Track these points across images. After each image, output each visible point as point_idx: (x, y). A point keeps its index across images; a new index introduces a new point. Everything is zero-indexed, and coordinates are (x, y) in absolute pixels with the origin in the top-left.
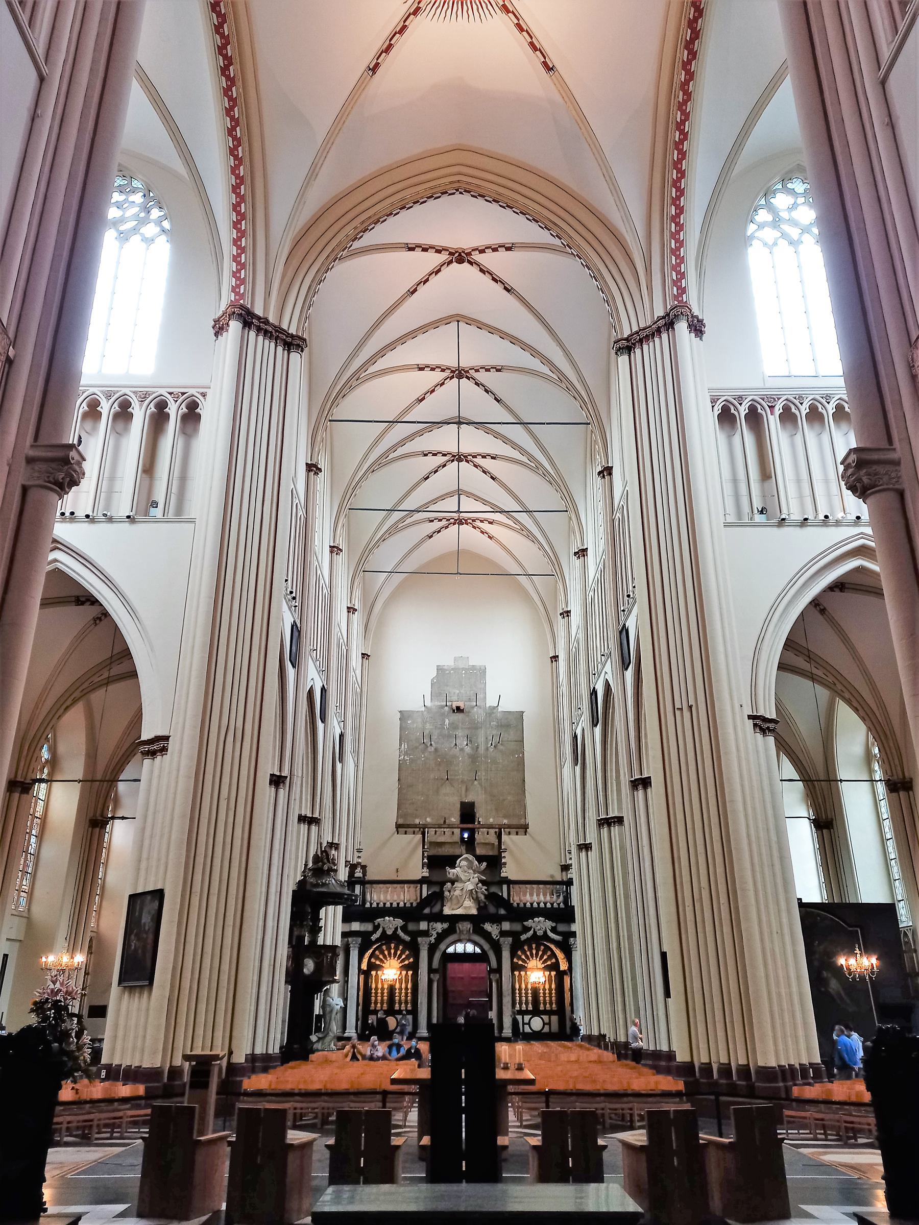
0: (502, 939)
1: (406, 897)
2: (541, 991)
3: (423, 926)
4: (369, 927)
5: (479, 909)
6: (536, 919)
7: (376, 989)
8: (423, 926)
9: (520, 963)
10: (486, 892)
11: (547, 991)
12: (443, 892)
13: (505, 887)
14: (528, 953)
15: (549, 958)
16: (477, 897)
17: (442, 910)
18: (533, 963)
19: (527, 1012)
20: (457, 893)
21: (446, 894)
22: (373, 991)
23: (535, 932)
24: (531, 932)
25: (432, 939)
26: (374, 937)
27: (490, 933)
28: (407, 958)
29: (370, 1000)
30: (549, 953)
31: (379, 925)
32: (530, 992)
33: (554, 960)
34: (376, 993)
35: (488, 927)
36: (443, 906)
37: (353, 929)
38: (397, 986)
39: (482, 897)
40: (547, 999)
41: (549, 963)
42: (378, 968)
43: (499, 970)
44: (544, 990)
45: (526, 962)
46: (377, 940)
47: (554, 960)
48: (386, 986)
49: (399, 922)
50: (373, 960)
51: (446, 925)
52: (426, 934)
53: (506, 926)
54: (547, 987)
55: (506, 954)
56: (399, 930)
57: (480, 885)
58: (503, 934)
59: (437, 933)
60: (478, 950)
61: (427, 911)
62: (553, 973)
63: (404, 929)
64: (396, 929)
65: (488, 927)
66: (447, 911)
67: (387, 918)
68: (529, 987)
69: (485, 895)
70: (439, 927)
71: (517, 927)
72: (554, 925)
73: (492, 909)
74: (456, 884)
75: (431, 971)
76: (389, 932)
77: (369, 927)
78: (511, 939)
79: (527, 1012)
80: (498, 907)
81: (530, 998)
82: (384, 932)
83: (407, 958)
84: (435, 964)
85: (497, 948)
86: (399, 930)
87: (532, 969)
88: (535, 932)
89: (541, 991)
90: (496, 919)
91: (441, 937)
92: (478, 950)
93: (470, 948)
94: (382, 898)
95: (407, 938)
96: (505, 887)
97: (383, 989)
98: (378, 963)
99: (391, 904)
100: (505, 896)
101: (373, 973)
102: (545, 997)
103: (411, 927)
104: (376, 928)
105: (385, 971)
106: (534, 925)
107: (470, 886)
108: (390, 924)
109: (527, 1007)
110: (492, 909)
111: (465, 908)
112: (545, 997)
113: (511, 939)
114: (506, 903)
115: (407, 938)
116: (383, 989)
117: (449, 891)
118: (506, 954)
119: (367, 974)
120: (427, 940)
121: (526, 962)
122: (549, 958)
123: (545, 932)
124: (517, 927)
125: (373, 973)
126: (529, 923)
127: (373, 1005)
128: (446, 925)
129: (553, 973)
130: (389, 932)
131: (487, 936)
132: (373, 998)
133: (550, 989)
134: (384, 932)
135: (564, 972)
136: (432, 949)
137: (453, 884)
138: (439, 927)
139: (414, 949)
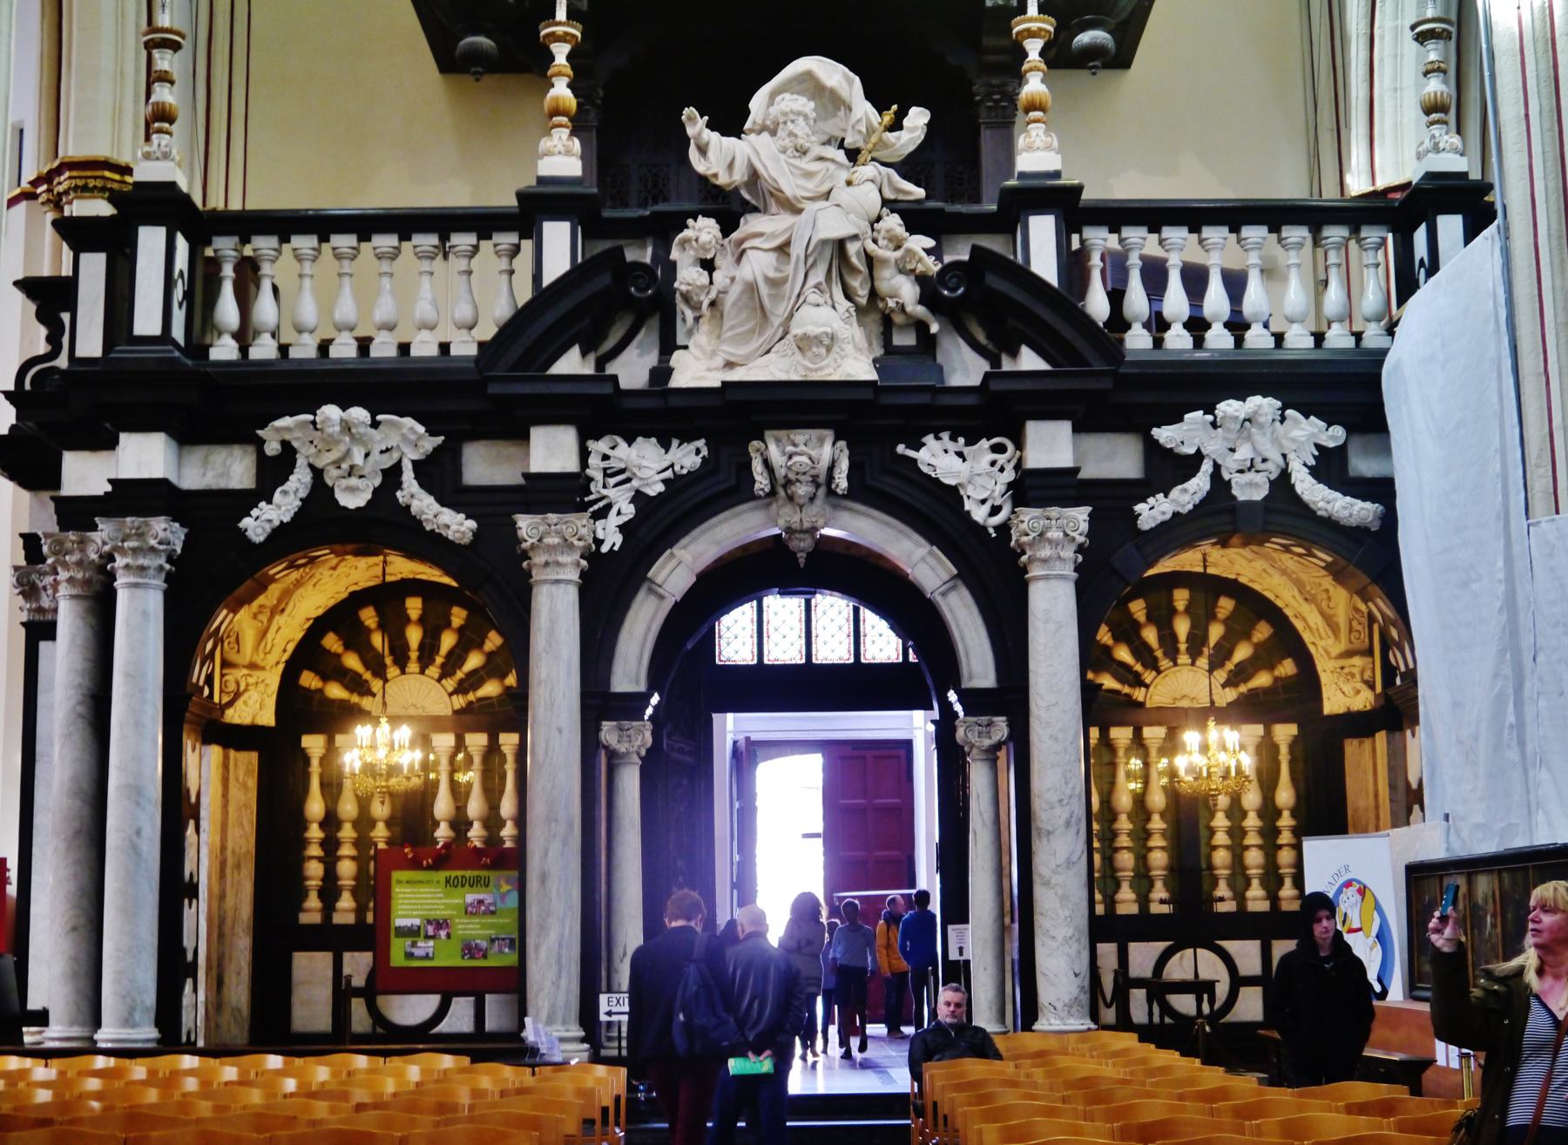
0: (1029, 518)
1: (451, 305)
2: (1220, 821)
3: (552, 450)
4: (231, 468)
5: (889, 356)
6: (1228, 408)
7: (331, 822)
8: (552, 450)
9: (1108, 682)
10: (932, 266)
11: (1252, 821)
12: (672, 266)
13: (1042, 230)
14: (1150, 635)
15: (1263, 658)
16: (874, 294)
17: (661, 373)
18: (1183, 682)
19: (1144, 927)
20: (759, 264)
21: (688, 275)
22: (315, 833)
23: (1219, 484)
24: (1199, 484)
25: (610, 535)
26: (258, 524)
27: (951, 496)
28: (493, 668)
29: (299, 877)
30: (1262, 632)
31: (288, 453)
32: (1157, 824)
33: (1287, 668)
34: (330, 845)
35: (938, 457)
36: (668, 345)
37: (128, 472)
38: (443, 806)
39: (907, 292)
40: (1254, 858)
41: (1262, 680)
42: (333, 719)
43: (1010, 697)
44: (1236, 811)
45: (1138, 682)
46: (281, 534)
47: (1287, 668)
48: (380, 810)
49: (408, 438)
50: (309, 680)
51: (687, 457)
52: (565, 493)
53: (1050, 445)
54: (1252, 799)
55: (1052, 607)
56: (408, 476)
57: (893, 222)
58: (1033, 488)
59: (639, 498)
60: (883, 644)
61: (572, 363)
62: (1285, 733)
63: (439, 474)
64: (392, 476)
65: (938, 457)
66: (695, 369)
67: (330, 412)
68: (1157, 800)
69: (922, 280)
70: (650, 463)
71: (1116, 458)
72: (1334, 436)
73: (964, 367)
74: (750, 224)
75: (599, 703)
76: (353, 497)
77: (231, 468)
78: (1080, 517)
79: (1144, 927)
80: (998, 345)
81: (1158, 859)
82: (320, 491)
83: (493, 668)
84: (629, 669)
85: (997, 575)
86: (408, 476)
87: (1174, 719)
88: (1219, 484)
89: (1220, 821)
90: (994, 415)
91: (660, 521)
92: (883, 644)
93: (836, 629)
94: (308, 311)
95: (458, 526)
96: (1042, 230)
97: (364, 822)
98: (335, 691)
99: (364, 344)
100: (1045, 266)
101: (313, 744)
102: (1238, 850)
103: (483, 465)
104: (274, 471)
105: (362, 731)
106: (1213, 446)
107: (833, 225)
108: (357, 450)
109: (1144, 900)
110: (964, 367)
111: (805, 343)
112: (1238, 850)
113: (1080, 517)
114: (1049, 314)
115: (458, 526)
116: (364, 822)
117: (708, 265)
118: (1052, 607)
119: (278, 756)
120: (578, 525)
121: (1138, 682)
122: (1263, 658)
123: (1282, 483)
124: (1116, 458)
125: (313, 744)
126: (1183, 434)
127: (313, 902)
128: (687, 457)
129: (1285, 733)
130: (353, 497)
131: (935, 511)
132: (314, 870)
133: (1269, 812)
134: (320, 491)
135: (1358, 725)
136: (607, 587)
137: (728, 225)
138: (650, 463)
139: (490, 588)
